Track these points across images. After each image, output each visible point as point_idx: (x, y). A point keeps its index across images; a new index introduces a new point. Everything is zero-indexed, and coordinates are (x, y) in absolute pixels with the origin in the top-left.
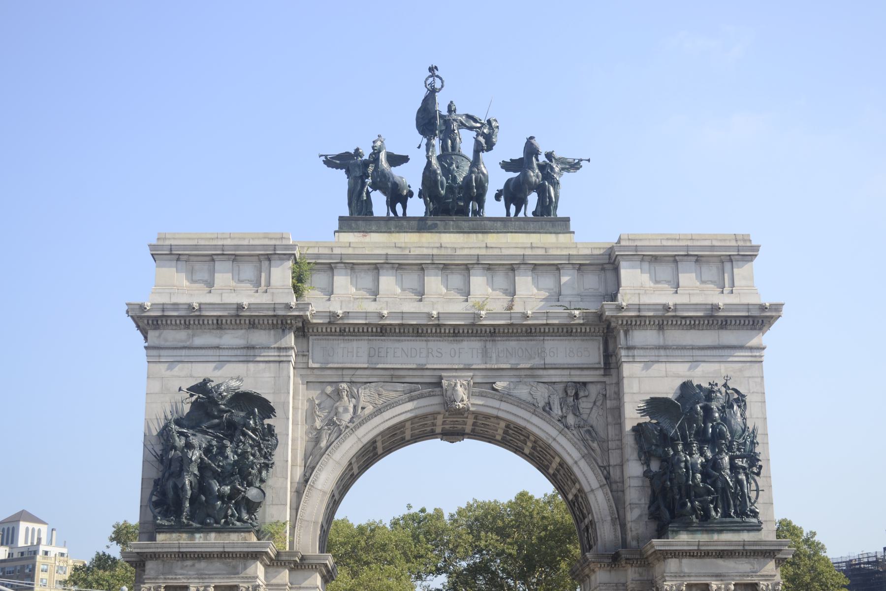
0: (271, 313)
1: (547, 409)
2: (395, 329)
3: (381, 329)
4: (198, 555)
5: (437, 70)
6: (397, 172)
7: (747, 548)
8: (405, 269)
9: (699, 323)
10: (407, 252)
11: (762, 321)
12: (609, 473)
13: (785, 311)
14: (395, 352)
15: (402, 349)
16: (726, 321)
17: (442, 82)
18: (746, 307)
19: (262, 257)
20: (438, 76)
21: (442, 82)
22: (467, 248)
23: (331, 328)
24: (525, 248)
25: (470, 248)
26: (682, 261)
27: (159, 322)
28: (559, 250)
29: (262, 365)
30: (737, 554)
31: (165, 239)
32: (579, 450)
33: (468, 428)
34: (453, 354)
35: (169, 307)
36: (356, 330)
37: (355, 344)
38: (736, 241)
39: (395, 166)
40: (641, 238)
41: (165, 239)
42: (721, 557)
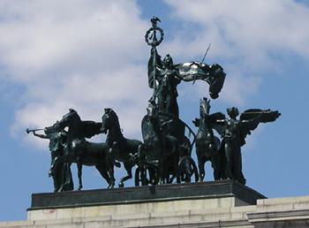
17: (162, 35)
20: (159, 29)
21: (162, 35)
24: (182, 217)
25: (136, 220)
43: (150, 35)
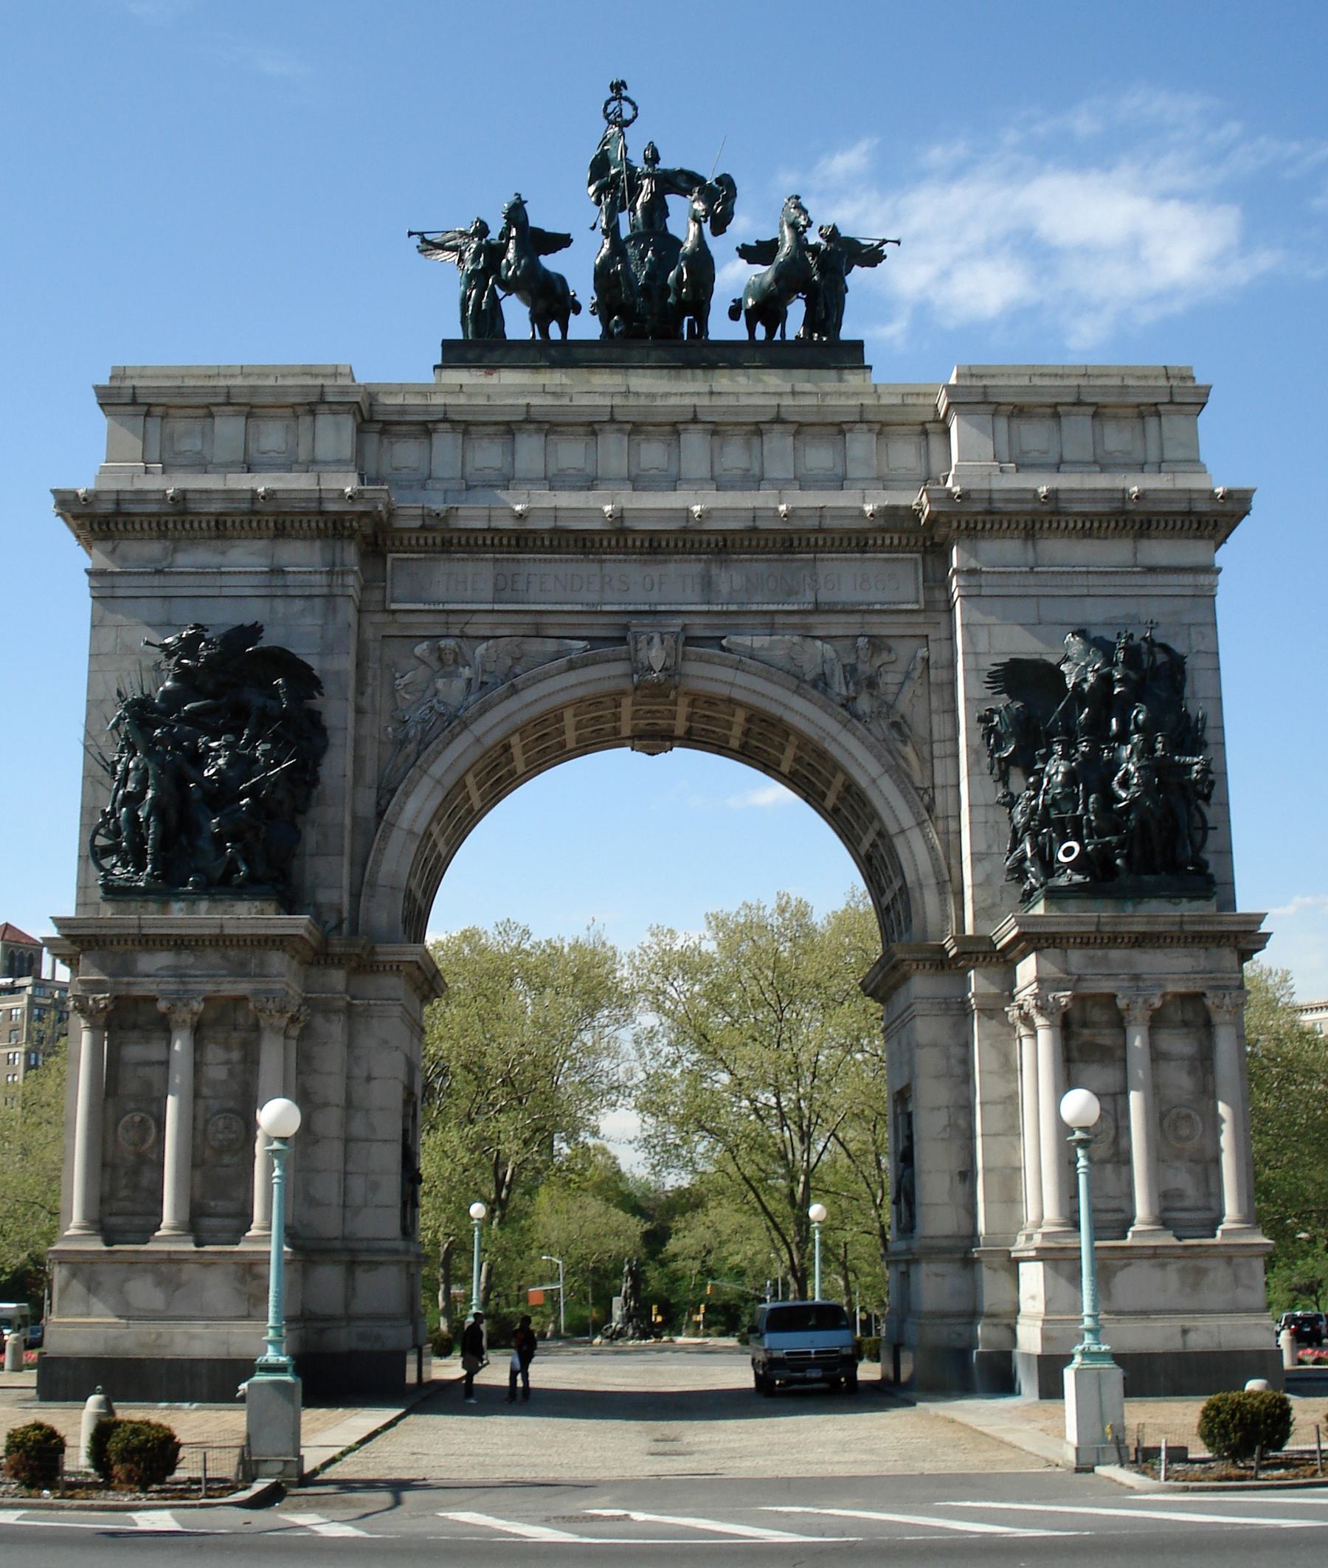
0: (313, 506)
1: (821, 685)
2: (543, 539)
3: (518, 540)
4: (176, 941)
5: (626, 88)
6: (550, 262)
7: (1187, 928)
8: (562, 433)
9: (1100, 526)
10: (565, 401)
11: (1216, 521)
12: (933, 799)
13: (1256, 501)
14: (542, 583)
15: (556, 577)
16: (1150, 522)
17: (636, 109)
18: (1187, 496)
19: (300, 410)
20: (627, 99)
22: (676, 394)
23: (426, 539)
25: (681, 394)
26: (1068, 414)
27: (112, 526)
28: (843, 398)
29: (299, 604)
30: (1169, 940)
31: (124, 378)
32: (878, 757)
33: (680, 727)
34: (649, 587)
35: (128, 496)
36: (472, 541)
37: (470, 568)
38: (1168, 378)
39: (546, 254)
40: (992, 372)
41: (124, 378)
42: (1139, 946)
43: (609, 111)
